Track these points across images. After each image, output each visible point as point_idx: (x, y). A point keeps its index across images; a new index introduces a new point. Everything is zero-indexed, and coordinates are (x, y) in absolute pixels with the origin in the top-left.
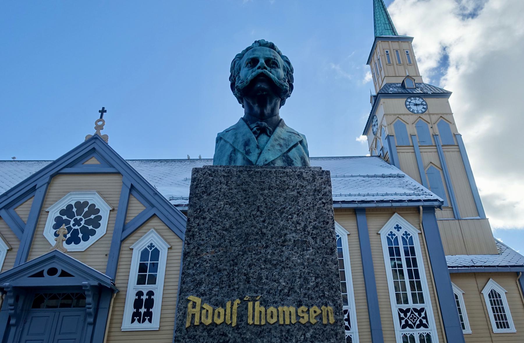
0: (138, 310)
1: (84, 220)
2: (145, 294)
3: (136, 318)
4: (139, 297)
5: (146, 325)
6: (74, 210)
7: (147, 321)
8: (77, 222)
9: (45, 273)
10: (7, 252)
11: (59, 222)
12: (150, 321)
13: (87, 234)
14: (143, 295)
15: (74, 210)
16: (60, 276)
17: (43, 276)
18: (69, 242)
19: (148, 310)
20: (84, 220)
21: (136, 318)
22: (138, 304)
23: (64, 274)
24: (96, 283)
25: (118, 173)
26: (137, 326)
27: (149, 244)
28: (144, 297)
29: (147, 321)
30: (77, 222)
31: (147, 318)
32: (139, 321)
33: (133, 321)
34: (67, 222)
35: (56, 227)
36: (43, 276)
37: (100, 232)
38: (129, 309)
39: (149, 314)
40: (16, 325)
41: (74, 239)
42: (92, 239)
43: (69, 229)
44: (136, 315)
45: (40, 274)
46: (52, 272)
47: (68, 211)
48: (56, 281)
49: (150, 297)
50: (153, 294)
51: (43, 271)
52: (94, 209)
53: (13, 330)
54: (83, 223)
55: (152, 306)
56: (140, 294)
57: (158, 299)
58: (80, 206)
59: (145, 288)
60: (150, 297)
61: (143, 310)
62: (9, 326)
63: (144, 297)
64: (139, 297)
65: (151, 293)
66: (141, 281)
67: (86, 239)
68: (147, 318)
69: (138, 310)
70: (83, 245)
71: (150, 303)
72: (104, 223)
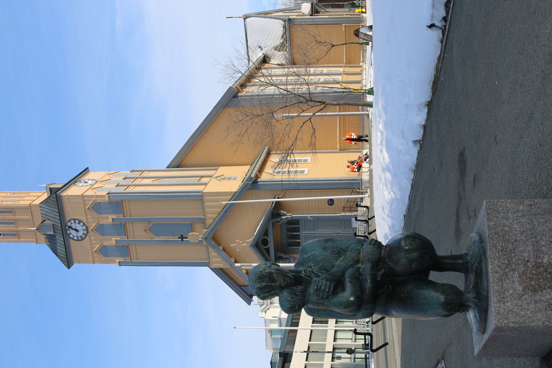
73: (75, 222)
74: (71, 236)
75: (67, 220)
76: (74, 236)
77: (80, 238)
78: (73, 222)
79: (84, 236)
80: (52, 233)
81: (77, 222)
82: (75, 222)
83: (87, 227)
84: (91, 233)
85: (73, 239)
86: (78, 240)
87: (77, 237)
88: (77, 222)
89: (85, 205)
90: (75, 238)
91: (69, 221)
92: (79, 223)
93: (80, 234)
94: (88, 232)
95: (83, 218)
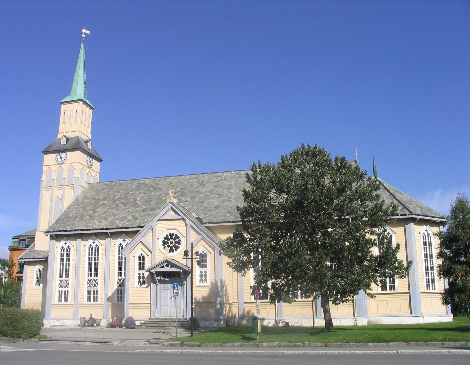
1: (174, 242)
3: (201, 282)
4: (201, 273)
5: (205, 284)
6: (169, 237)
7: (205, 282)
8: (172, 243)
9: (165, 266)
11: (164, 243)
12: (206, 282)
14: (202, 272)
15: (169, 237)
16: (171, 267)
17: (164, 267)
18: (170, 251)
20: (174, 242)
21: (201, 282)
22: (201, 276)
26: (201, 284)
27: (202, 251)
28: (203, 273)
29: (205, 282)
31: (205, 282)
32: (202, 282)
33: (200, 282)
34: (168, 243)
35: (164, 245)
36: (164, 267)
38: (198, 278)
39: (206, 280)
41: (171, 251)
43: (168, 246)
44: (201, 280)
45: (163, 267)
46: (167, 266)
47: (166, 238)
51: (164, 266)
54: (174, 243)
56: (201, 272)
58: (171, 235)
59: (203, 270)
60: (205, 273)
61: (203, 278)
63: (203, 273)
64: (201, 273)
65: (205, 272)
68: (205, 282)
69: (201, 278)
70: (176, 253)
71: (205, 276)
73: (65, 157)
75: (66, 153)
77: (57, 159)
78: (66, 156)
79: (58, 162)
80: (61, 144)
81: (65, 158)
82: (65, 157)
84: (59, 165)
85: (57, 155)
86: (56, 158)
88: (65, 158)
89: (73, 163)
90: (57, 157)
91: (66, 154)
92: (65, 160)
94: (59, 164)
95: (66, 162)
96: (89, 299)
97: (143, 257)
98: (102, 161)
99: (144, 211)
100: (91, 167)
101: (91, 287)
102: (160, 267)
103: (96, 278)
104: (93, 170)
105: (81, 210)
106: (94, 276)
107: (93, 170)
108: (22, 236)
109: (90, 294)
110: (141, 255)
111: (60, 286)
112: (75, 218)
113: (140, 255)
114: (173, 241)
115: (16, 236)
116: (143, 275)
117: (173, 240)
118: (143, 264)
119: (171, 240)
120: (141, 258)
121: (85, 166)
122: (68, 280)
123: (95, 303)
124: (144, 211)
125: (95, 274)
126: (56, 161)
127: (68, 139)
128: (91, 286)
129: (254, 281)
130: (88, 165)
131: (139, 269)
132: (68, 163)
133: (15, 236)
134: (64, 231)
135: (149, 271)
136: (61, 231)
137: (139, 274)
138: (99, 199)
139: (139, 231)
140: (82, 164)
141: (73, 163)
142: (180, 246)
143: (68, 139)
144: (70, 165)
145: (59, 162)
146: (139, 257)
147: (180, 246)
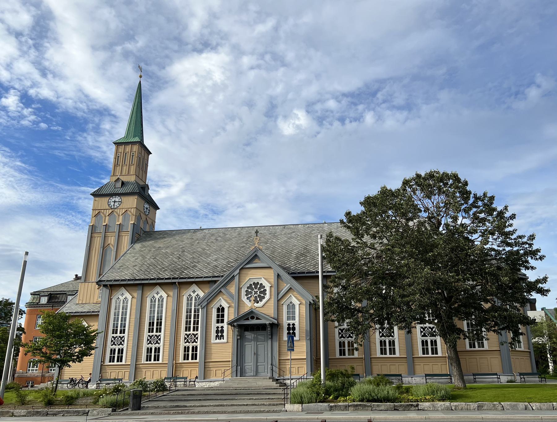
0: (289, 332)
2: (291, 325)
4: (289, 326)
8: (256, 293)
10: (228, 309)
11: (247, 293)
13: (262, 298)
19: (293, 331)
23: (257, 319)
24: (271, 323)
25: (270, 268)
28: (291, 326)
30: (256, 293)
37: (267, 297)
40: (240, 339)
42: (264, 301)
45: (248, 319)
46: (253, 318)
47: (250, 287)
48: (255, 322)
49: (293, 326)
50: (295, 325)
52: (262, 286)
53: (239, 341)
54: (258, 293)
55: (295, 330)
57: (297, 326)
58: (256, 284)
60: (293, 326)
62: (237, 339)
64: (289, 326)
66: (288, 318)
67: (261, 300)
69: (289, 332)
70: (261, 304)
72: (268, 292)
74: (111, 198)
76: (111, 200)
81: (120, 203)
83: (116, 209)
86: (108, 202)
87: (110, 202)
90: (110, 201)
91: (121, 198)
93: (112, 204)
96: (148, 358)
97: (223, 309)
98: (159, 209)
99: (216, 260)
100: (148, 215)
101: (152, 344)
102: (244, 319)
103: (158, 334)
104: (149, 218)
105: (140, 258)
106: (157, 332)
107: (149, 218)
108: (44, 292)
109: (151, 352)
110: (221, 306)
111: (112, 343)
112: (134, 266)
113: (219, 306)
114: (257, 291)
115: (36, 292)
116: (222, 329)
117: (257, 290)
118: (223, 316)
119: (256, 290)
120: (221, 310)
121: (142, 212)
122: (123, 337)
123: (156, 362)
124: (216, 260)
125: (157, 329)
126: (109, 205)
127: (123, 183)
128: (152, 342)
129: (339, 336)
130: (145, 212)
131: (218, 322)
132: (123, 209)
133: (34, 292)
134: (122, 280)
135: (231, 324)
136: (118, 280)
137: (218, 327)
138: (160, 247)
139: (218, 281)
140: (139, 210)
141: (129, 208)
142: (265, 296)
143: (123, 183)
144: (126, 210)
145: (112, 206)
146: (218, 309)
147: (265, 296)
